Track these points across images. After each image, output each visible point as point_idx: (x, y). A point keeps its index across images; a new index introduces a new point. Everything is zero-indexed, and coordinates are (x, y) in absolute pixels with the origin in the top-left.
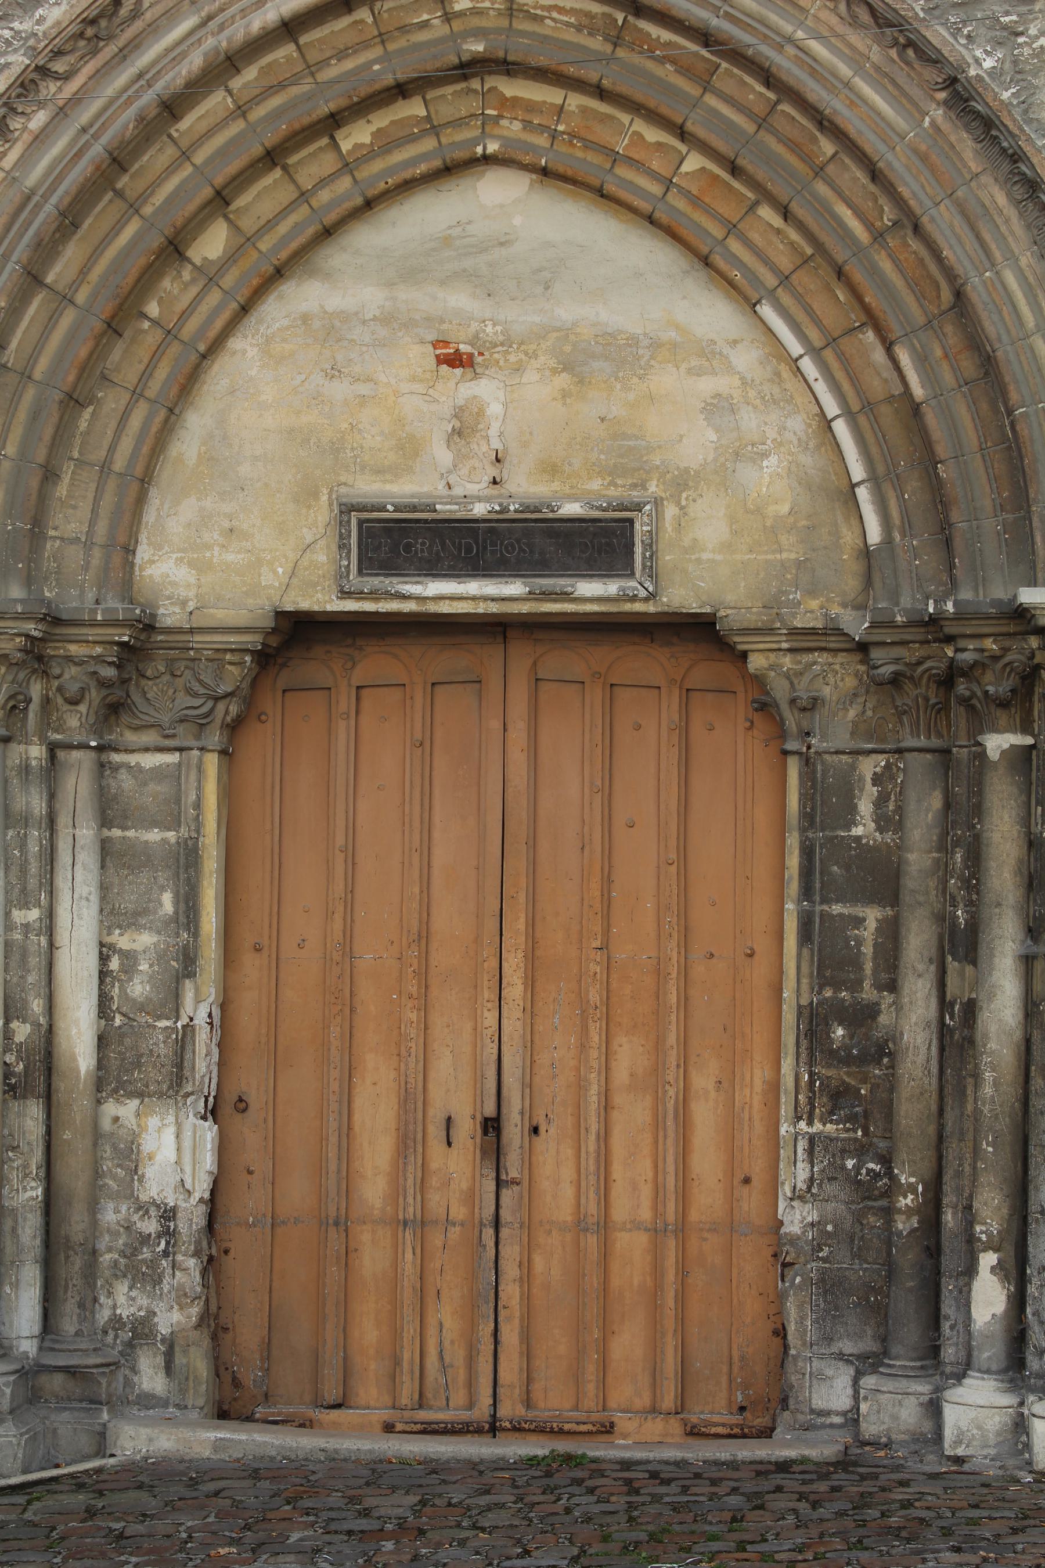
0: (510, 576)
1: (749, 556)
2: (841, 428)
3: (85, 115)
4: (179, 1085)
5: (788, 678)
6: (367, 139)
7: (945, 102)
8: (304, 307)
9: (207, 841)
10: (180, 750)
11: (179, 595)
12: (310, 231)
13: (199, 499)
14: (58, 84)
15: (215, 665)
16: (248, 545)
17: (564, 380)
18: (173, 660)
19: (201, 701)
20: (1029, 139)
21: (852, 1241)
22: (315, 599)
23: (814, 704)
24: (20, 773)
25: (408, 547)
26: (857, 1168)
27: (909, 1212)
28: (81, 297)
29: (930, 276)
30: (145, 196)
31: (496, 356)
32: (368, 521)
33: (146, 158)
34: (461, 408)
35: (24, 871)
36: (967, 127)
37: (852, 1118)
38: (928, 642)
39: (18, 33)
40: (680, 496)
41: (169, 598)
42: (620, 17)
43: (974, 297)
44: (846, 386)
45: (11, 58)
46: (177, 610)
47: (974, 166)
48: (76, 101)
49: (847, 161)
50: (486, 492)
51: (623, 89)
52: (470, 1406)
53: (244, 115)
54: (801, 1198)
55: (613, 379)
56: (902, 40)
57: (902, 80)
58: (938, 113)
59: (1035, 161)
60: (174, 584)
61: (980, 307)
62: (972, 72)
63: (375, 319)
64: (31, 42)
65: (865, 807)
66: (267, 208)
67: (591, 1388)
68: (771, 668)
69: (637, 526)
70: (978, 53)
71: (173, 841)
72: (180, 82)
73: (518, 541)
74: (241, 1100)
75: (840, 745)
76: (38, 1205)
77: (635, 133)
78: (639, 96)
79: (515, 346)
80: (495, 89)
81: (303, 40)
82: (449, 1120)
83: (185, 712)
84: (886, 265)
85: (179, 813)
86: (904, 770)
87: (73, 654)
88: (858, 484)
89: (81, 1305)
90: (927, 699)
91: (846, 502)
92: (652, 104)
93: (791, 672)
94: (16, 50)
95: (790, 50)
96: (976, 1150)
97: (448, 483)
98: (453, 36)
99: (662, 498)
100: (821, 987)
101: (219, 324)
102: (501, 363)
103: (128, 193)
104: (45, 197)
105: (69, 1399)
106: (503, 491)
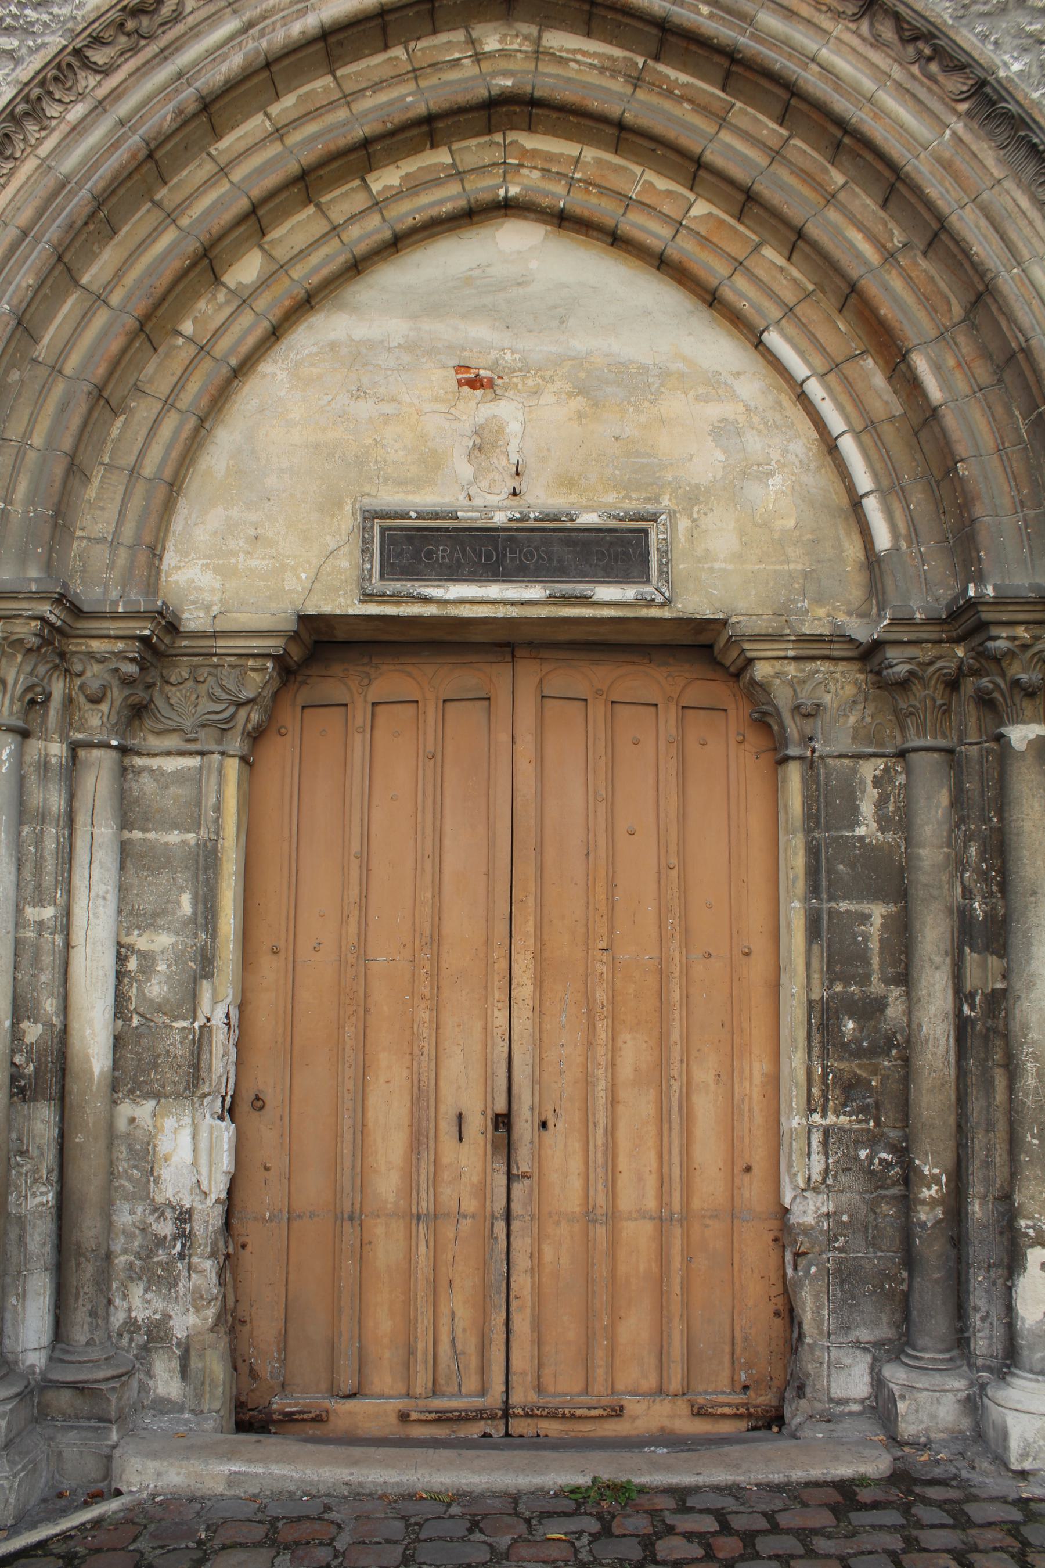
0: (529, 581)
1: (757, 567)
3: (123, 108)
4: (196, 1086)
5: (792, 686)
6: (396, 182)
7: (968, 113)
8: (332, 336)
9: (226, 844)
10: (202, 754)
11: (203, 600)
13: (225, 509)
14: (98, 78)
15: (237, 671)
17: (578, 403)
18: (196, 667)
19: (224, 706)
21: (867, 1230)
22: (337, 603)
23: (811, 713)
24: (38, 769)
25: (429, 554)
26: (870, 1158)
27: (933, 1202)
28: (115, 299)
29: (940, 292)
31: (515, 380)
32: (390, 529)
33: (185, 173)
35: (39, 867)
36: (991, 136)
37: (864, 1109)
41: (194, 602)
42: (640, 61)
45: (47, 39)
46: (202, 615)
47: (997, 172)
48: (116, 95)
49: (857, 189)
50: (505, 503)
52: (483, 1393)
53: (281, 138)
56: (927, 51)
57: (922, 94)
58: (959, 127)
60: (199, 589)
63: (399, 346)
64: (70, 25)
65: (867, 808)
66: (300, 240)
68: (777, 675)
69: (652, 536)
71: (193, 842)
73: (537, 549)
74: (258, 1098)
77: (646, 181)
79: (533, 372)
82: (460, 1116)
83: (207, 716)
84: (897, 284)
85: (200, 816)
87: (95, 650)
89: (93, 1313)
90: (934, 700)
93: (795, 680)
94: (53, 32)
95: (814, 67)
97: (469, 495)
99: (675, 512)
100: (832, 982)
102: (520, 386)
103: (166, 203)
104: (80, 185)
105: (77, 1417)
106: (522, 502)
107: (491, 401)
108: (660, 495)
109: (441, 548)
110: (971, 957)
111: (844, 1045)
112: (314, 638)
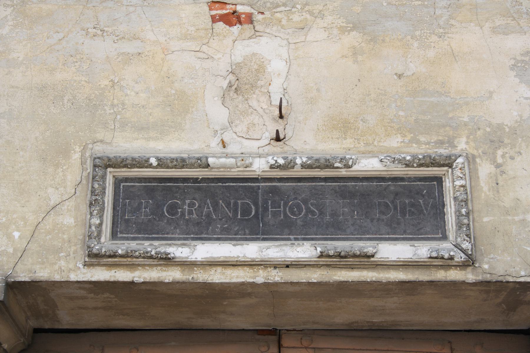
0: (296, 239)
22: (57, 267)
25: (173, 209)
31: (278, 15)
34: (238, 64)
40: (494, 155)
50: (267, 149)
55: (409, 37)
69: (447, 184)
73: (305, 202)
79: (299, 7)
97: (223, 142)
99: (474, 157)
102: (284, 22)
106: (286, 148)
107: (250, 38)
108: (454, 138)
109: (188, 202)
112: (33, 323)
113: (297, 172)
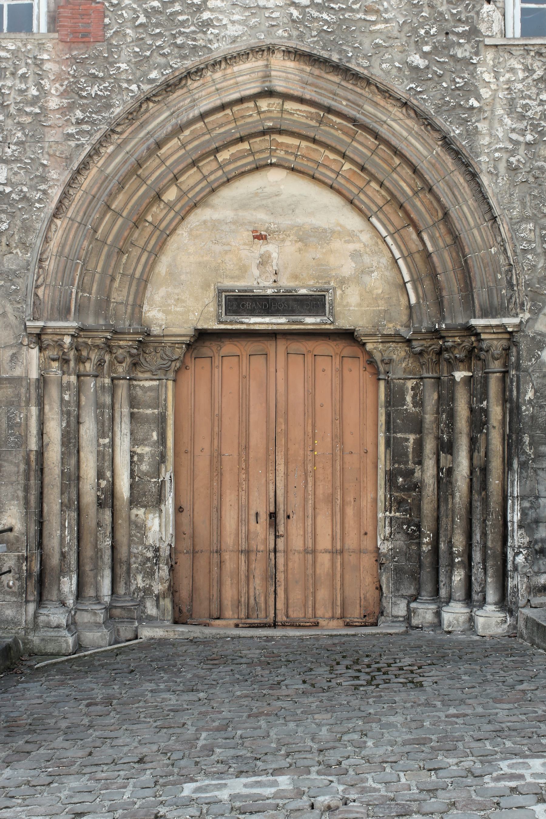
2: (401, 262)
3: (128, 148)
6: (228, 157)
7: (442, 145)
8: (204, 218)
10: (159, 380)
12: (208, 190)
16: (184, 304)
17: (300, 244)
20: (472, 159)
23: (390, 362)
25: (243, 305)
27: (427, 544)
28: (125, 214)
29: (434, 207)
30: (148, 177)
33: (148, 163)
35: (103, 424)
36: (449, 154)
37: (405, 511)
38: (433, 339)
39: (104, 117)
42: (322, 114)
43: (452, 215)
44: (403, 247)
45: (102, 127)
47: (452, 168)
48: (126, 141)
49: (404, 166)
51: (323, 139)
52: (266, 617)
53: (184, 148)
54: (387, 540)
56: (426, 123)
58: (439, 149)
59: (475, 166)
60: (157, 319)
61: (454, 219)
62: (452, 135)
63: (230, 222)
64: (109, 120)
65: (409, 399)
66: (192, 182)
67: (310, 610)
68: (375, 348)
69: (327, 297)
70: (454, 128)
72: (163, 135)
74: (181, 508)
75: (399, 376)
76: (109, 547)
78: (329, 142)
80: (274, 139)
81: (206, 121)
82: (257, 514)
84: (419, 204)
86: (423, 385)
88: (407, 282)
89: (126, 584)
91: (402, 289)
92: (334, 145)
94: (103, 124)
95: (385, 126)
96: (453, 521)
98: (261, 120)
101: (174, 224)
103: (142, 176)
104: (113, 177)
105: (123, 618)
110: (442, 455)
111: (398, 487)
113: (281, 294)
